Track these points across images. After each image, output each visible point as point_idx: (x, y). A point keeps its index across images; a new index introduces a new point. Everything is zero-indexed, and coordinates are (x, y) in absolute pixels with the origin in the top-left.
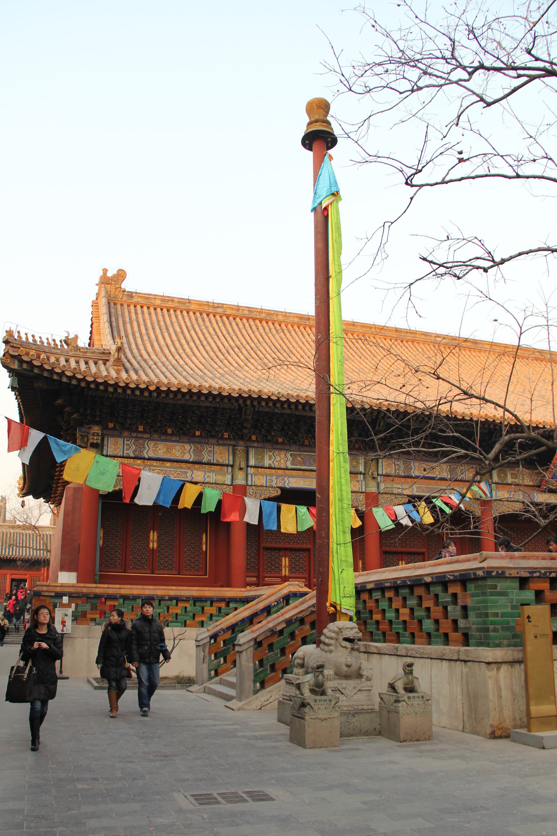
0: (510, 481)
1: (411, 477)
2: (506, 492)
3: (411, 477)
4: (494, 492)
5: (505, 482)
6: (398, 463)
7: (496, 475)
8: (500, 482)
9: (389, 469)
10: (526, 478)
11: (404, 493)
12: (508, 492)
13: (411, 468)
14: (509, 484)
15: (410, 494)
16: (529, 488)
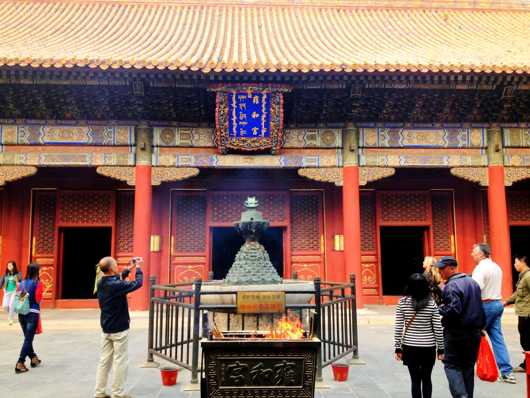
0: (178, 142)
1: (40, 145)
2: (171, 156)
3: (40, 145)
4: (154, 157)
5: (171, 144)
6: (22, 129)
7: (158, 136)
8: (163, 144)
9: (9, 137)
10: (202, 138)
11: (29, 163)
12: (174, 156)
13: (39, 134)
14: (177, 147)
15: (37, 163)
16: (209, 149)
